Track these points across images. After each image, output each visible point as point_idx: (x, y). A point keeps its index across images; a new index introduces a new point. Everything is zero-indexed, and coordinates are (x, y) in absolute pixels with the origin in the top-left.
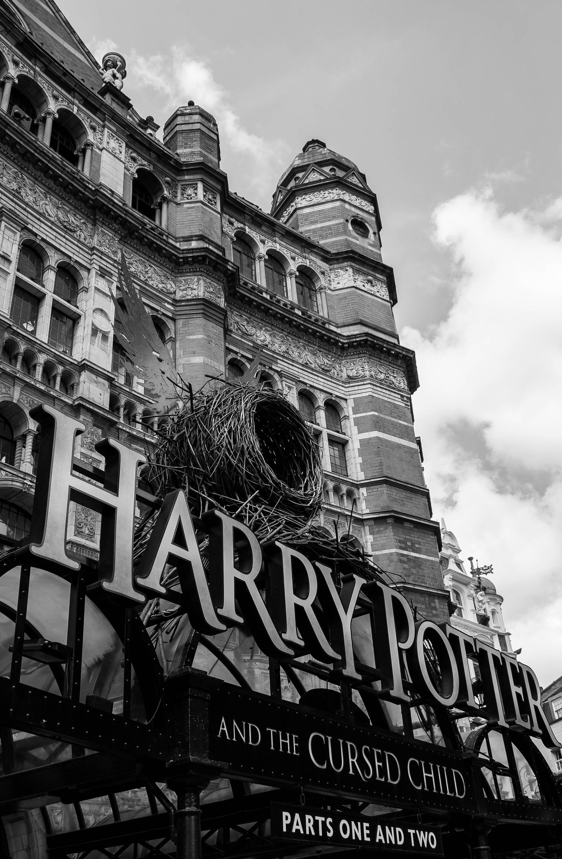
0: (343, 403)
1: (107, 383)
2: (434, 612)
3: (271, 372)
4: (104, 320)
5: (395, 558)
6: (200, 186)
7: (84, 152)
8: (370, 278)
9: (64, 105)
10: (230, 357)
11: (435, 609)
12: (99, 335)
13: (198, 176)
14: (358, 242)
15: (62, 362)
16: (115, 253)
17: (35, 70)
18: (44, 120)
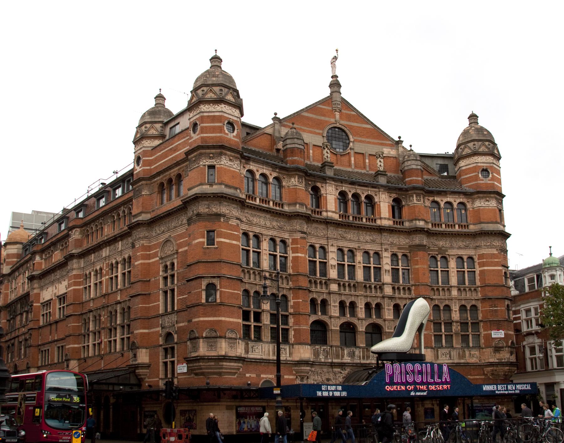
9: (365, 194)
13: (413, 192)
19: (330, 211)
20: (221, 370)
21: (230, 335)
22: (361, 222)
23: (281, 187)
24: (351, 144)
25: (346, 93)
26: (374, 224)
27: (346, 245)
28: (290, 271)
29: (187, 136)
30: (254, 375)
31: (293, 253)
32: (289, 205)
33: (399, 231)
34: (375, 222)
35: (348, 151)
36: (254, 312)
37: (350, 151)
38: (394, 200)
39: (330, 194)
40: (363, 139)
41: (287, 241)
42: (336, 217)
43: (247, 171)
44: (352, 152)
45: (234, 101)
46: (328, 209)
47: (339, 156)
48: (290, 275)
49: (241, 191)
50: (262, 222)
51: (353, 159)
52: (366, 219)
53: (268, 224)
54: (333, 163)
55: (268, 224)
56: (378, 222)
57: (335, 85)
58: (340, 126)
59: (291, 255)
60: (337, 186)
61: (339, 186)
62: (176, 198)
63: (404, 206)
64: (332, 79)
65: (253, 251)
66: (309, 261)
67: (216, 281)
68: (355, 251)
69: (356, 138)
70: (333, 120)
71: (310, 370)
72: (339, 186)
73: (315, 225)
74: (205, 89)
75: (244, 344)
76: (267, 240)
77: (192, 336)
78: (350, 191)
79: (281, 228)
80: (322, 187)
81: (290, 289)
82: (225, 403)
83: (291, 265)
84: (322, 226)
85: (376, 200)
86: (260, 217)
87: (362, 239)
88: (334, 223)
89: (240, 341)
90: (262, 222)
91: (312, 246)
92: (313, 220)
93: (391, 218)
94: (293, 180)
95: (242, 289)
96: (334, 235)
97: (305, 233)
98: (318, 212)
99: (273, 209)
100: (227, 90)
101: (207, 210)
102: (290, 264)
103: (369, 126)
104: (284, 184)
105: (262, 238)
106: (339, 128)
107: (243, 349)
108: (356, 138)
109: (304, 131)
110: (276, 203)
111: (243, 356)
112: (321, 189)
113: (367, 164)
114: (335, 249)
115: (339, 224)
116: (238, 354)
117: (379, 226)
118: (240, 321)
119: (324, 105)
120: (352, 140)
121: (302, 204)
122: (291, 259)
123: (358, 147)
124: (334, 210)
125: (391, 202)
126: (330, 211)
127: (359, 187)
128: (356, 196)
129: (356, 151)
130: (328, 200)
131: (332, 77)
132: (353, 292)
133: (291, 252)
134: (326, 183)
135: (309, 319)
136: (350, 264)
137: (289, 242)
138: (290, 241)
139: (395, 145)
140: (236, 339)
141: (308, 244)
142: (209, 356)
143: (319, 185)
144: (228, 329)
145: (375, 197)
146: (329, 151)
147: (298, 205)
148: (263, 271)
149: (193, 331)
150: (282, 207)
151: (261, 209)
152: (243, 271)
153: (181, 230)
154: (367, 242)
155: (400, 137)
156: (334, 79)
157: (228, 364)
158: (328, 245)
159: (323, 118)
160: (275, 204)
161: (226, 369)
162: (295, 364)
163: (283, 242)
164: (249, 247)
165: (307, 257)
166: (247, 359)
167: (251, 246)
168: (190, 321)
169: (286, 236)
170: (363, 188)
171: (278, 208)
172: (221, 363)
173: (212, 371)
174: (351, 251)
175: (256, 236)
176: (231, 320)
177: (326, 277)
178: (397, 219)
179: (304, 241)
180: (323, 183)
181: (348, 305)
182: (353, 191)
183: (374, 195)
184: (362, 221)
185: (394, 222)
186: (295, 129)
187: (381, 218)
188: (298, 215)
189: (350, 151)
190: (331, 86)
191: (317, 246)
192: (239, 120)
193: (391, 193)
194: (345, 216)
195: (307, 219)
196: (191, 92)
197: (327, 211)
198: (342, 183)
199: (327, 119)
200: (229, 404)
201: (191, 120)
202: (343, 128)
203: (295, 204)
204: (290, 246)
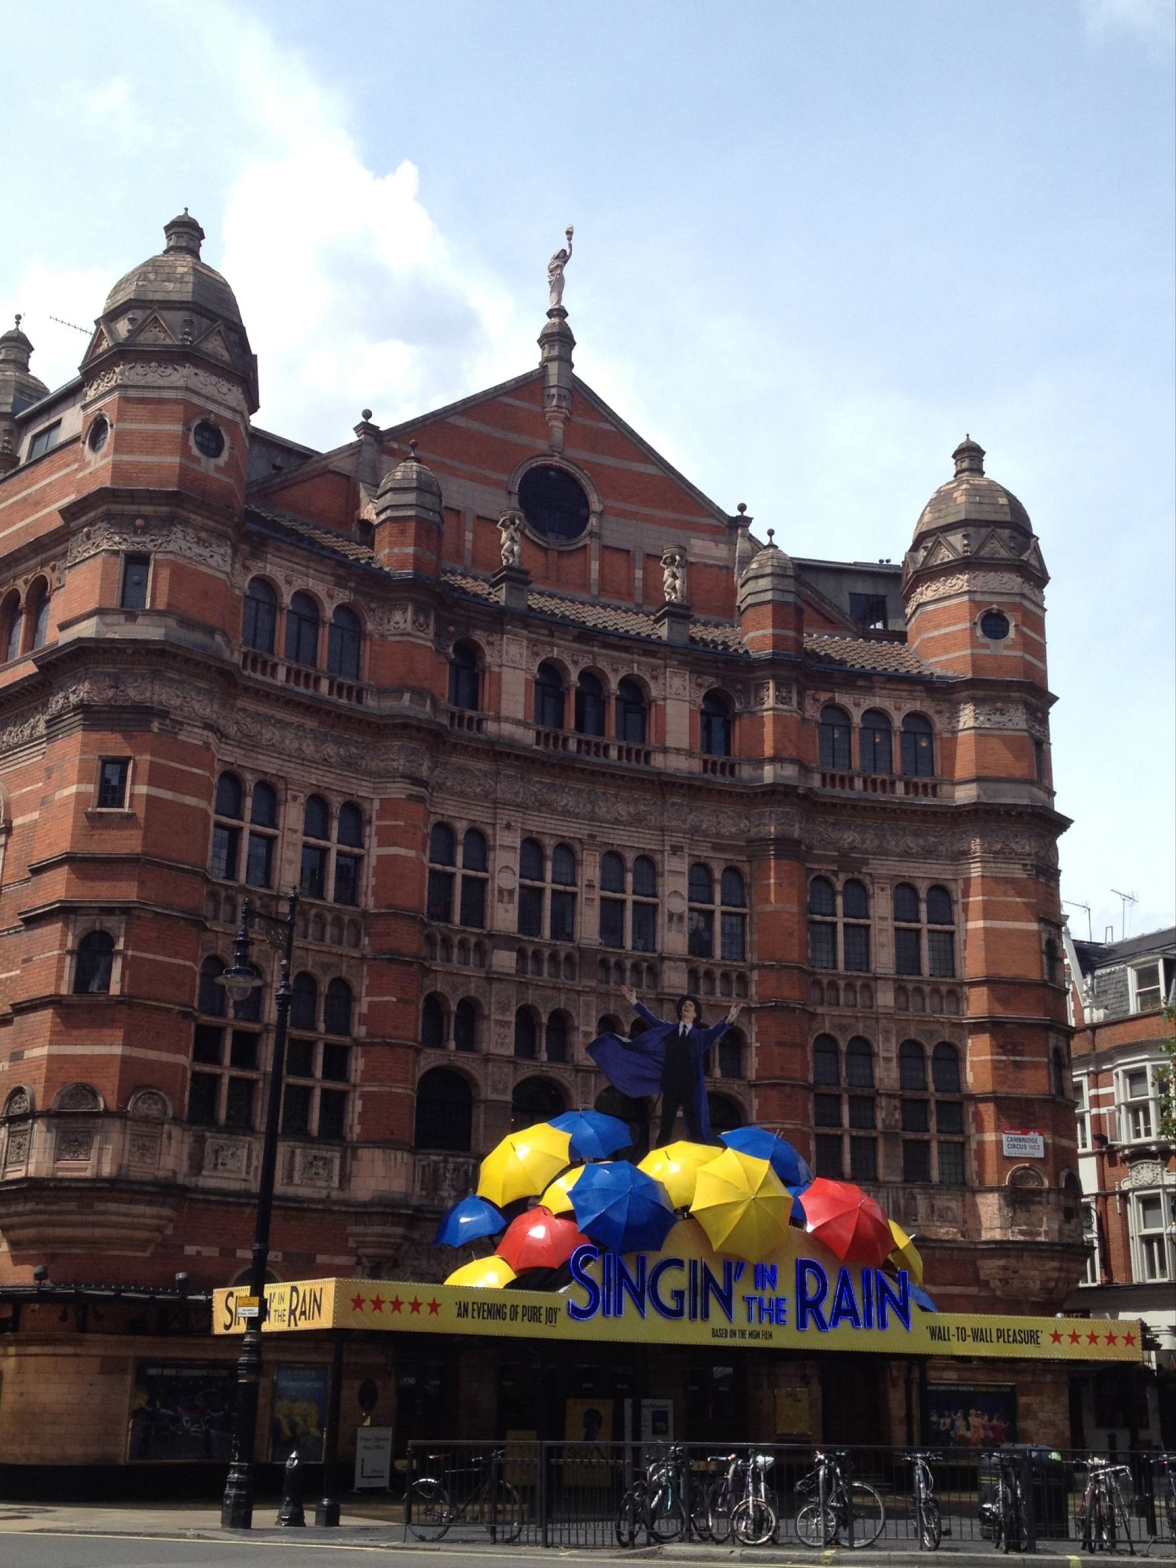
0: (952, 886)
1: (684, 965)
3: (861, 877)
4: (681, 901)
5: (989, 1065)
6: (771, 685)
7: (650, 705)
8: (999, 705)
9: (623, 673)
10: (813, 876)
12: (675, 918)
13: (769, 672)
14: (988, 652)
15: (646, 960)
16: (684, 821)
17: (592, 653)
18: (609, 698)
19: (507, 720)
20: (98, 1232)
22: (602, 760)
23: (358, 635)
24: (593, 521)
25: (587, 366)
26: (642, 766)
27: (551, 828)
28: (368, 902)
29: (76, 460)
30: (213, 1252)
31: (380, 845)
32: (381, 692)
33: (719, 792)
34: (647, 761)
35: (584, 540)
36: (237, 1034)
37: (588, 541)
38: (706, 698)
39: (512, 668)
40: (633, 508)
41: (366, 805)
42: (527, 736)
43: (253, 579)
44: (594, 545)
45: (226, 356)
46: (504, 712)
47: (553, 556)
48: (365, 914)
49: (228, 642)
50: (290, 742)
51: (595, 566)
52: (620, 750)
53: (309, 748)
54: (527, 573)
55: (309, 748)
56: (658, 761)
57: (558, 340)
58: (564, 465)
59: (374, 850)
60: (533, 643)
61: (543, 643)
62: (24, 651)
63: (740, 715)
64: (547, 320)
65: (253, 833)
66: (433, 872)
67: (111, 923)
68: (577, 847)
69: (609, 503)
70: (541, 445)
71: (405, 1238)
72: (543, 643)
73: (457, 760)
74: (139, 314)
75: (189, 1139)
76: (302, 799)
77: (17, 1110)
78: (575, 663)
79: (349, 764)
80: (490, 644)
81: (363, 958)
83: (373, 881)
84: (484, 765)
85: (654, 693)
86: (283, 725)
87: (602, 810)
88: (517, 757)
89: (176, 1132)
91: (444, 829)
92: (455, 745)
93: (697, 750)
94: (398, 616)
95: (203, 955)
96: (517, 793)
98: (471, 719)
99: (327, 702)
100: (206, 322)
101: (110, 693)
102: (368, 879)
103: (651, 470)
104: (370, 626)
106: (560, 471)
107: (185, 1156)
108: (609, 503)
109: (452, 472)
110: (340, 687)
111: (181, 1180)
112: (487, 650)
113: (639, 584)
114: (515, 840)
115: (534, 761)
117: (659, 774)
118: (184, 1060)
119: (517, 398)
120: (596, 506)
121: (419, 693)
122: (373, 861)
123: (618, 532)
124: (520, 716)
125: (700, 700)
126: (507, 720)
127: (604, 651)
128: (592, 678)
129: (607, 542)
130: (504, 687)
131: (550, 314)
133: (375, 840)
134: (503, 633)
135: (416, 1062)
136: (560, 887)
138: (376, 805)
139: (727, 531)
141: (433, 819)
142: (62, 1180)
143: (479, 636)
144: (137, 1088)
145: (652, 684)
146: (518, 536)
147: (407, 696)
148: (278, 898)
149: (20, 1091)
150: (359, 700)
152: (213, 895)
153: (30, 759)
154: (617, 821)
155: (742, 508)
156: (556, 320)
157: (124, 1208)
158: (494, 825)
159: (512, 437)
160: (338, 688)
161: (115, 1226)
162: (357, 1214)
164: (241, 819)
165: (426, 859)
166: (196, 1189)
167: (248, 815)
168: (16, 1057)
169: (363, 789)
170: (616, 654)
171: (344, 701)
172: (100, 1206)
173: (69, 1232)
174: (565, 848)
176: (152, 1055)
177: (482, 926)
178: (719, 758)
180: (491, 631)
181: (545, 1019)
182: (586, 662)
183: (647, 678)
184: (606, 754)
185: (705, 762)
186: (418, 460)
187: (665, 750)
188: (405, 726)
189: (588, 541)
190: (545, 340)
191: (461, 827)
192: (238, 419)
193: (700, 674)
194: (556, 738)
195: (434, 739)
196: (97, 322)
197: (498, 719)
198: (551, 635)
199: (524, 440)
201: (89, 410)
202: (572, 469)
203: (398, 692)
204: (375, 823)
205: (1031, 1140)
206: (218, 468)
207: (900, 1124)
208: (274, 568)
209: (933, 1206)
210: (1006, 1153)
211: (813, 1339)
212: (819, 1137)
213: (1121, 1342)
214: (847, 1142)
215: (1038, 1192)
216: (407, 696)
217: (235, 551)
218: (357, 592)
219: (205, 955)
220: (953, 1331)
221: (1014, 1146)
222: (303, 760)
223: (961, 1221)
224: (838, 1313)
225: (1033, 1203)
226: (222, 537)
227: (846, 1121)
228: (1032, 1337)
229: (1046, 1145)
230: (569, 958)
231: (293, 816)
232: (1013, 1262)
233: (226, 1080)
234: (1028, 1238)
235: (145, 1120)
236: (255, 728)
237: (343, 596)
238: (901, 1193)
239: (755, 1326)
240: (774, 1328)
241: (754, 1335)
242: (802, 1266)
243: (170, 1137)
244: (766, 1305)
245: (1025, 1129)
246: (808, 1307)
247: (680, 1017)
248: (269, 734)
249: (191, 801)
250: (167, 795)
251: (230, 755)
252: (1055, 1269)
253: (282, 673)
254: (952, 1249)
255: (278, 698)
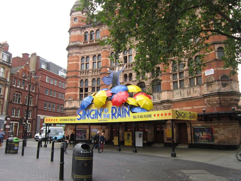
2: (211, 66)
11: (211, 65)
21: (69, 99)
36: (85, 88)
48: (101, 69)
53: (92, 50)
55: (92, 50)
79: (98, 50)
81: (100, 75)
82: (69, 127)
90: (90, 50)
97: (106, 48)
105: (90, 57)
116: (72, 107)
132: (130, 68)
137: (101, 54)
140: (72, 101)
141: (110, 52)
151: (88, 46)
157: (68, 111)
161: (68, 113)
163: (99, 55)
169: (100, 52)
175: (88, 57)
176: (71, 93)
179: (105, 52)
200: (71, 127)
205: (211, 71)
206: (77, 22)
207: (188, 75)
208: (87, 30)
209: (194, 90)
210: (206, 75)
211: (115, 120)
212: (173, 82)
213: (168, 115)
214: (178, 82)
215: (213, 82)
216: (106, 37)
217: (81, 31)
218: (98, 27)
219: (80, 80)
220: (137, 116)
221: (207, 73)
222: (92, 52)
223: (200, 92)
224: (118, 115)
225: (212, 85)
226: (78, 30)
227: (178, 78)
228: (150, 116)
229: (214, 71)
230: (132, 65)
231: (91, 59)
232: (208, 99)
233: (84, 94)
234: (211, 93)
235: (70, 101)
236: (85, 51)
237: (96, 29)
238: (188, 89)
239: (105, 119)
240: (108, 119)
241: (105, 120)
242: (112, 107)
243: (73, 102)
244: (107, 115)
245: (210, 68)
246: (113, 115)
247: (115, 71)
248: (87, 50)
249: (74, 62)
250: (72, 63)
251: (82, 55)
252: (217, 99)
253: (89, 42)
254: (199, 98)
255: (86, 46)
